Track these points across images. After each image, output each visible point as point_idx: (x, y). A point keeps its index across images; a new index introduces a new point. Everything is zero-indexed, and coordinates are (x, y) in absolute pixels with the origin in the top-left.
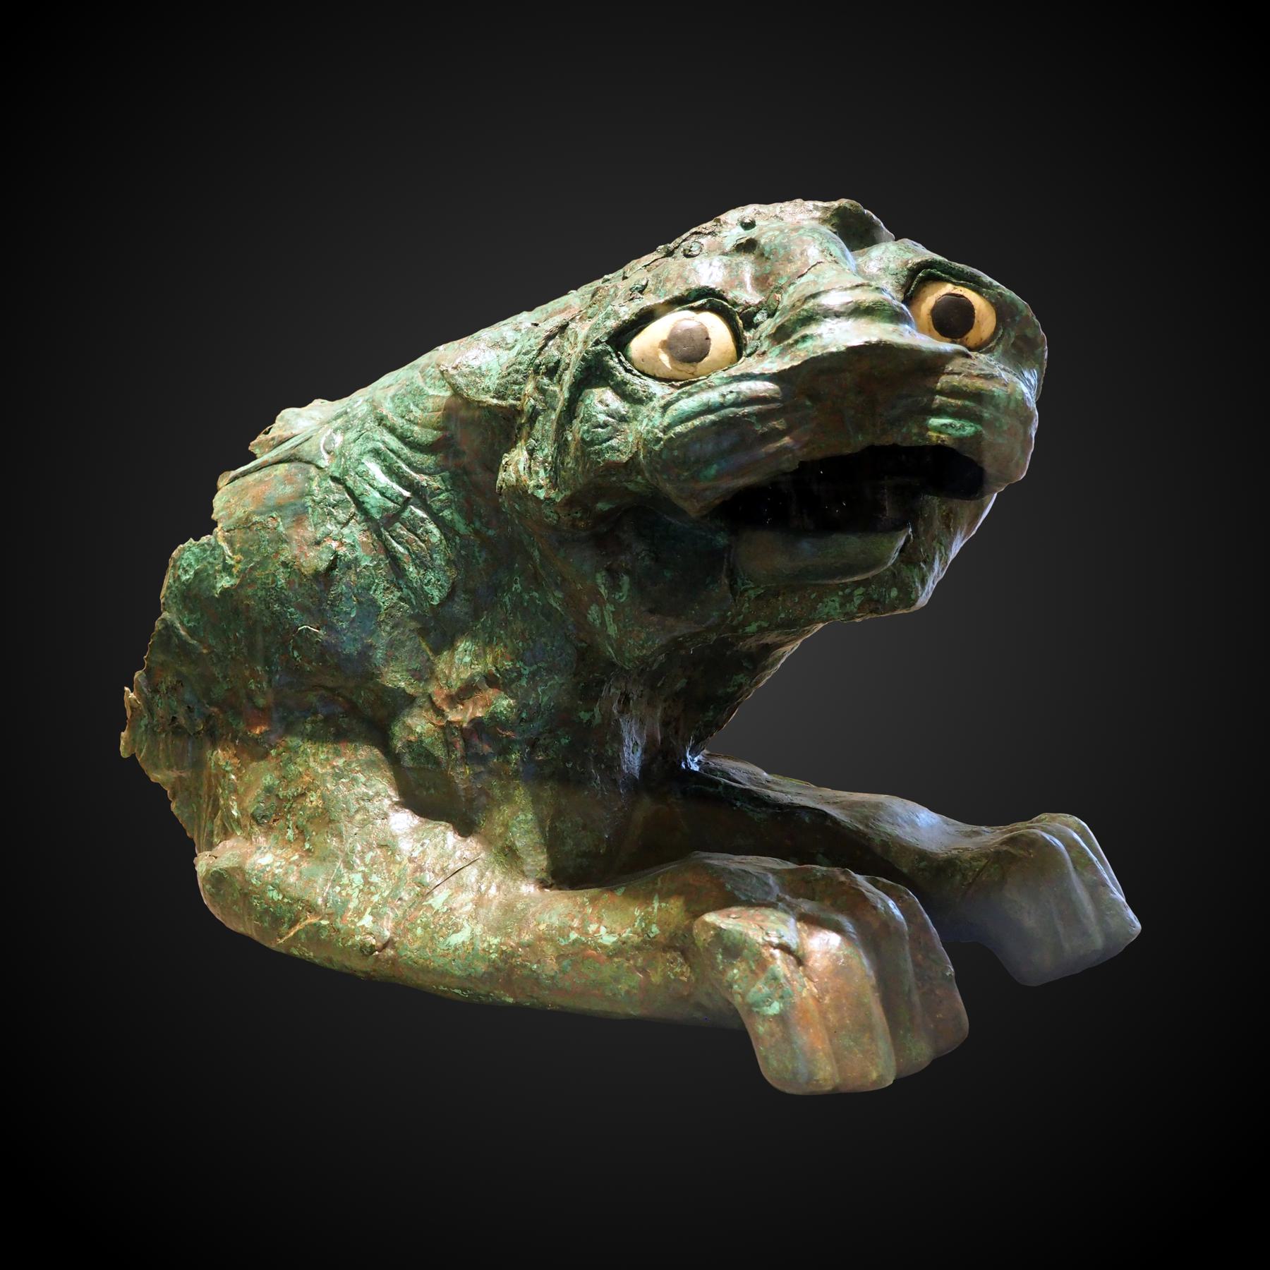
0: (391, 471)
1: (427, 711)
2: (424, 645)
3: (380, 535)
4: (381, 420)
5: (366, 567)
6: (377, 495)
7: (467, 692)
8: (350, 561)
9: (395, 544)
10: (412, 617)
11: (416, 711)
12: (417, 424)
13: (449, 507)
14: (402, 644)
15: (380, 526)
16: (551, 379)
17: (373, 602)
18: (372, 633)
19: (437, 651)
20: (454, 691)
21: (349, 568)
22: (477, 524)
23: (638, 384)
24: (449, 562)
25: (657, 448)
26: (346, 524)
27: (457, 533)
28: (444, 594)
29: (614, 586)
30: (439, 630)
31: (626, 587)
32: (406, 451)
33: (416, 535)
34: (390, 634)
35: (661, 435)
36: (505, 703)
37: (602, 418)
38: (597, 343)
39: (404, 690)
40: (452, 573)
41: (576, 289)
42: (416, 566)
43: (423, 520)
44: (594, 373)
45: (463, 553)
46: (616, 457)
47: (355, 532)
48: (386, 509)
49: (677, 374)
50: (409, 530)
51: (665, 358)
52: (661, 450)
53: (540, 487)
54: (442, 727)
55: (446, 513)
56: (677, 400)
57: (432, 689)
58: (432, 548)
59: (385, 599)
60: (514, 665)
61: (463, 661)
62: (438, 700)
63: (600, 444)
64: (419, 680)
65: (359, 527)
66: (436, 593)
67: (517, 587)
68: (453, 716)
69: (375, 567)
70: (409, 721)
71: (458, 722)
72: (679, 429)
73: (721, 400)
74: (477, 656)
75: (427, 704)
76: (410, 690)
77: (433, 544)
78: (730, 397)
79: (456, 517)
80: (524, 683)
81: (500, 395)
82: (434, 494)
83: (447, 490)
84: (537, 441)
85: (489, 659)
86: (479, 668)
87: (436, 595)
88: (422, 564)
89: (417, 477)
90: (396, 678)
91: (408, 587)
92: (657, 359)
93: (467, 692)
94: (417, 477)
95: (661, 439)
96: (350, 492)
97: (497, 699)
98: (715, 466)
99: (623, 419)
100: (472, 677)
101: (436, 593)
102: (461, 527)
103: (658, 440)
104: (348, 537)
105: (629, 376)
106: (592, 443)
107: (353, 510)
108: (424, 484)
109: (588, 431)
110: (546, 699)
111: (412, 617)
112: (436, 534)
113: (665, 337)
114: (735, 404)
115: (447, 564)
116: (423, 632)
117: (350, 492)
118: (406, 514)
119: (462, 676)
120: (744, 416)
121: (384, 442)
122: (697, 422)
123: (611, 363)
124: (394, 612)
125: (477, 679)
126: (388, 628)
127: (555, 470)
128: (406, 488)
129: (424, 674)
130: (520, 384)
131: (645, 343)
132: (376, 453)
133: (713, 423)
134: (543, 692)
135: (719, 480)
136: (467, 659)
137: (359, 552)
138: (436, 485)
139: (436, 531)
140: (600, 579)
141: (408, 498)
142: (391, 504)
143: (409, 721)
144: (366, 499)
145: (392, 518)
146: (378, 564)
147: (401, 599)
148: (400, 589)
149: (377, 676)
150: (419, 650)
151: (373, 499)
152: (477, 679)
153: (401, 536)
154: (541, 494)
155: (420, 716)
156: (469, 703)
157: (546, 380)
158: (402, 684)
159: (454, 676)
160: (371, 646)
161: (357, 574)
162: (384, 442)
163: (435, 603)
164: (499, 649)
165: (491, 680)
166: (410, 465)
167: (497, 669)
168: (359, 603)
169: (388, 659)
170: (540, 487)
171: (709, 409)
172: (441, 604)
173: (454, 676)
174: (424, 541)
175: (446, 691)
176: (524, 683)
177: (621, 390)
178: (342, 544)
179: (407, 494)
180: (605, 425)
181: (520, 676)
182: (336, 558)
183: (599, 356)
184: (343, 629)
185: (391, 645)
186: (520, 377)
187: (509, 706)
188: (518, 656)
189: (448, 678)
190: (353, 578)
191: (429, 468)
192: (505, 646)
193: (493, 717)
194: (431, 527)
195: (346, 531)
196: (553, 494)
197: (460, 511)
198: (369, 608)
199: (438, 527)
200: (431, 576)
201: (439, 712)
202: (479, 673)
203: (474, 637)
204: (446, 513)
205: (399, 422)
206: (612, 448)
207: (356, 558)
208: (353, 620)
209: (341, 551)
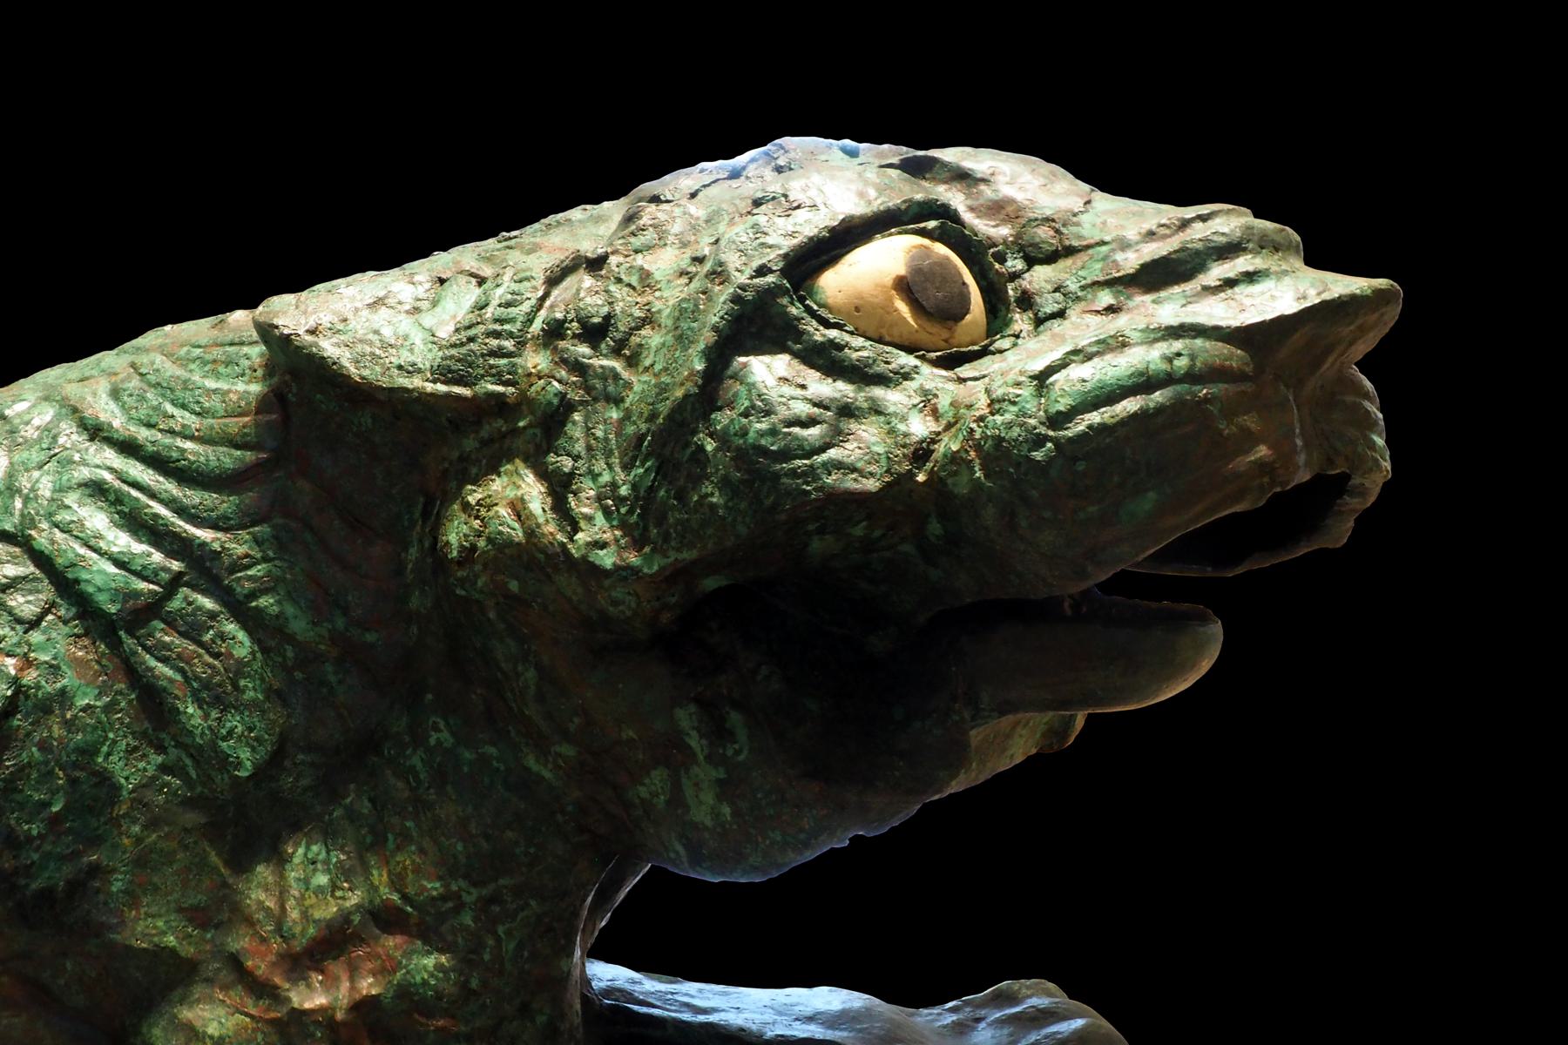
0: (135, 522)
1: (225, 988)
2: (214, 858)
3: (115, 645)
4: (96, 432)
5: (89, 706)
6: (111, 569)
7: (329, 947)
8: (50, 698)
9: (153, 663)
10: (189, 803)
11: (198, 990)
12: (192, 438)
13: (265, 591)
14: (169, 858)
15: (109, 626)
16: (595, 347)
17: (104, 779)
18: (95, 841)
19: (241, 863)
20: (298, 945)
21: (48, 711)
22: (340, 623)
23: (859, 349)
24: (269, 692)
25: (1038, 455)
26: (34, 624)
27: (290, 639)
28: (263, 752)
29: (718, 733)
30: (247, 824)
31: (742, 734)
32: (170, 487)
33: (201, 644)
34: (139, 840)
35: (1043, 430)
36: (430, 962)
37: (802, 409)
38: (762, 271)
39: (172, 952)
40: (276, 714)
41: (445, 249)
42: (200, 702)
43: (213, 616)
44: (759, 321)
45: (298, 675)
46: (851, 483)
47: (57, 642)
48: (136, 594)
49: (923, 338)
50: (182, 634)
51: (903, 308)
52: (1050, 461)
53: (603, 545)
54: (272, 1022)
55: (265, 601)
56: (1063, 365)
57: (239, 942)
58: (239, 670)
59: (129, 769)
60: (446, 886)
61: (307, 884)
62: (260, 965)
63: (808, 455)
64: (203, 926)
65: (66, 630)
66: (245, 754)
67: (442, 736)
68: (312, 997)
69: (109, 709)
70: (186, 1014)
71: (322, 1010)
72: (1095, 417)
73: (1164, 366)
74: (344, 873)
75: (226, 975)
76: (188, 951)
77: (239, 661)
78: (1182, 363)
79: (290, 610)
80: (467, 919)
81: (443, 373)
82: (236, 567)
83: (265, 559)
84: (576, 458)
85: (380, 877)
86: (354, 899)
87: (246, 759)
88: (215, 697)
89: (205, 535)
90: (155, 928)
91: (179, 745)
92: (889, 309)
93: (329, 947)
94: (205, 535)
95: (1046, 438)
96: (42, 560)
97: (408, 954)
98: (1152, 495)
99: (847, 411)
100: (345, 917)
101: (245, 754)
102: (299, 625)
103: (1040, 441)
104: (41, 648)
105: (833, 333)
106: (786, 455)
107: (47, 592)
108: (216, 546)
109: (773, 432)
110: (512, 946)
111: (189, 803)
112: (241, 643)
113: (902, 270)
114: (1191, 377)
115: (267, 698)
116: (213, 831)
117: (42, 560)
118: (176, 604)
119: (318, 914)
120: (1206, 400)
121: (111, 470)
122: (1130, 405)
123: (794, 311)
124: (149, 795)
125: (356, 919)
126: (136, 829)
127: (640, 518)
128: (170, 554)
129: (220, 911)
130: (510, 355)
131: (836, 282)
132: (96, 490)
133: (1160, 409)
134: (509, 933)
135: (1144, 528)
136: (322, 879)
137: (68, 680)
138: (241, 550)
139: (241, 635)
140: (686, 718)
141: (180, 574)
142: (143, 586)
143: (186, 1014)
144: (84, 576)
145: (143, 614)
146: (114, 703)
147: (164, 769)
148: (161, 749)
149: (111, 928)
150: (202, 865)
151: (100, 574)
152: (356, 919)
153: (167, 646)
154: (606, 558)
155: (211, 1000)
156: (337, 968)
157: (584, 349)
158: (171, 940)
159: (294, 914)
160: (95, 870)
161: (69, 725)
162: (111, 470)
163: (243, 774)
164: (406, 859)
165: (385, 919)
166: (181, 511)
167: (404, 897)
168: (73, 782)
169: (132, 897)
170: (603, 545)
171: (1144, 383)
172: (263, 773)
173: (294, 914)
174: (216, 656)
175: (276, 945)
176: (467, 919)
177: (827, 360)
178: (28, 663)
179: (176, 566)
180: (811, 422)
181: (459, 907)
182: (16, 694)
183: (770, 293)
184: (30, 839)
185: (141, 862)
186: (509, 344)
187: (439, 967)
188: (449, 868)
189: (280, 919)
190: (57, 731)
191: (225, 518)
192: (422, 851)
193: (405, 992)
194: (231, 627)
195: (36, 637)
196: (633, 558)
197: (290, 597)
198: (94, 796)
199: (245, 626)
200: (234, 722)
201: (261, 989)
202: (358, 907)
203: (329, 835)
204: (265, 601)
205: (143, 434)
206: (838, 465)
207: (63, 692)
208: (55, 820)
209: (30, 677)
